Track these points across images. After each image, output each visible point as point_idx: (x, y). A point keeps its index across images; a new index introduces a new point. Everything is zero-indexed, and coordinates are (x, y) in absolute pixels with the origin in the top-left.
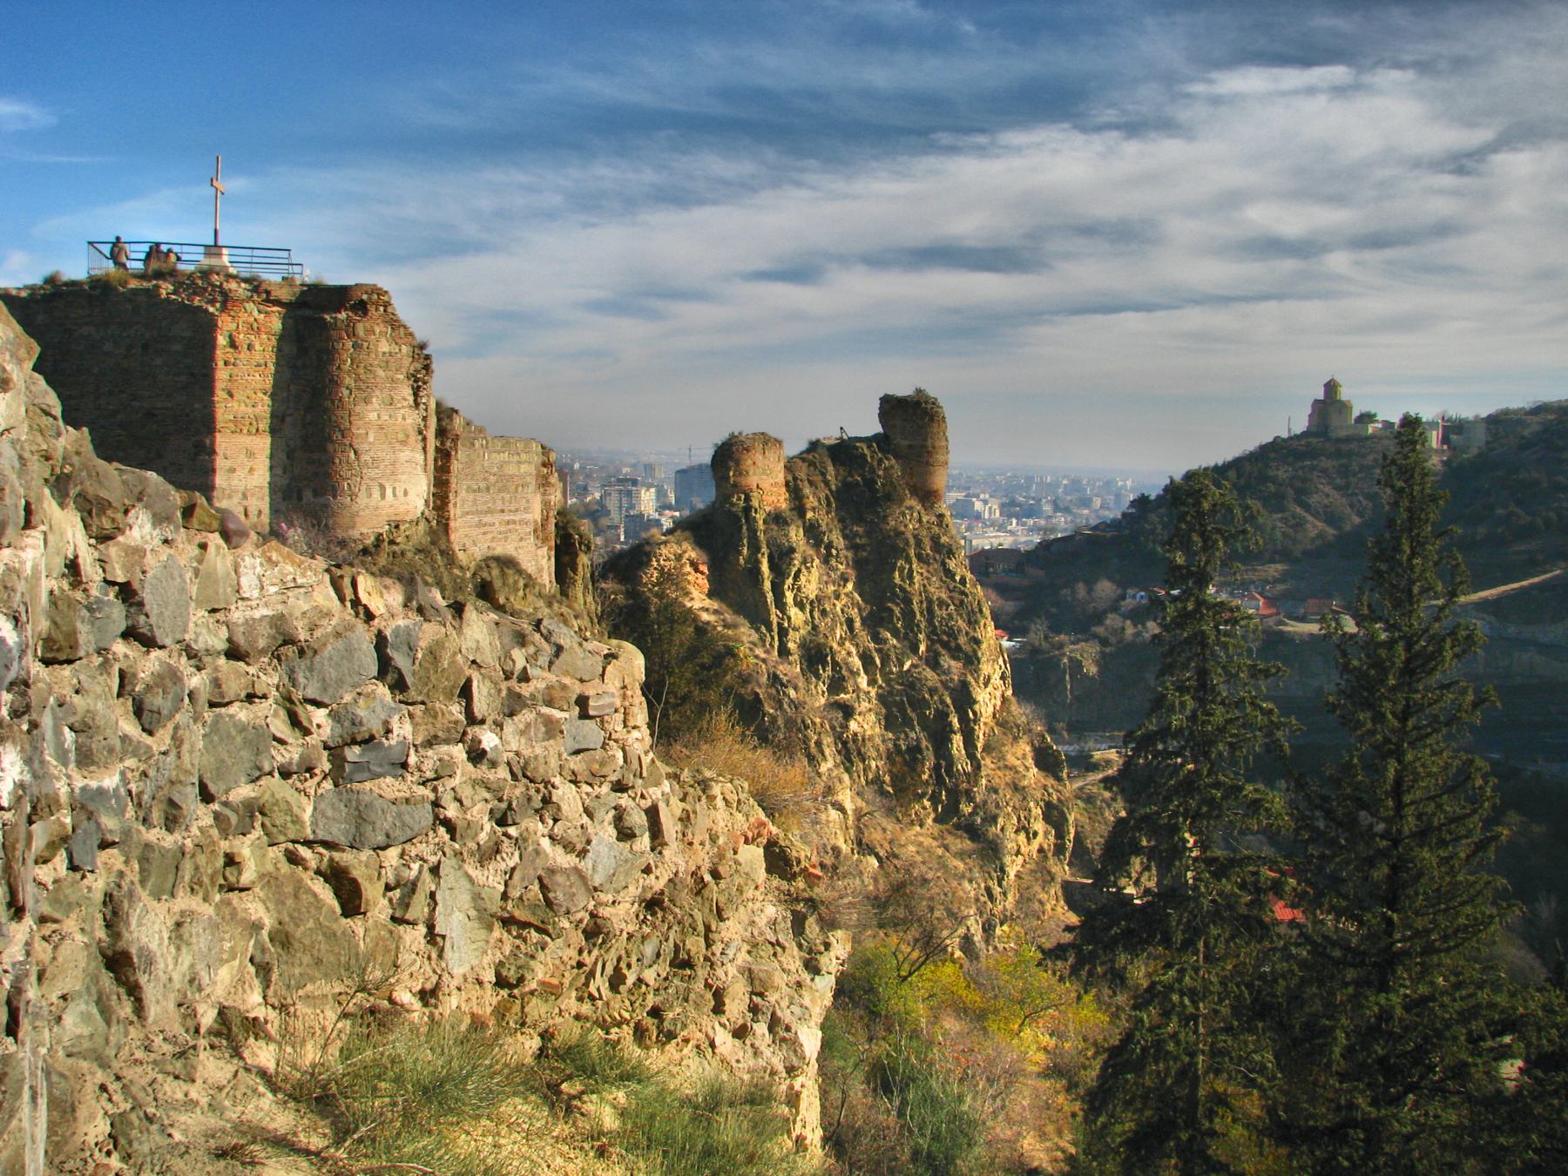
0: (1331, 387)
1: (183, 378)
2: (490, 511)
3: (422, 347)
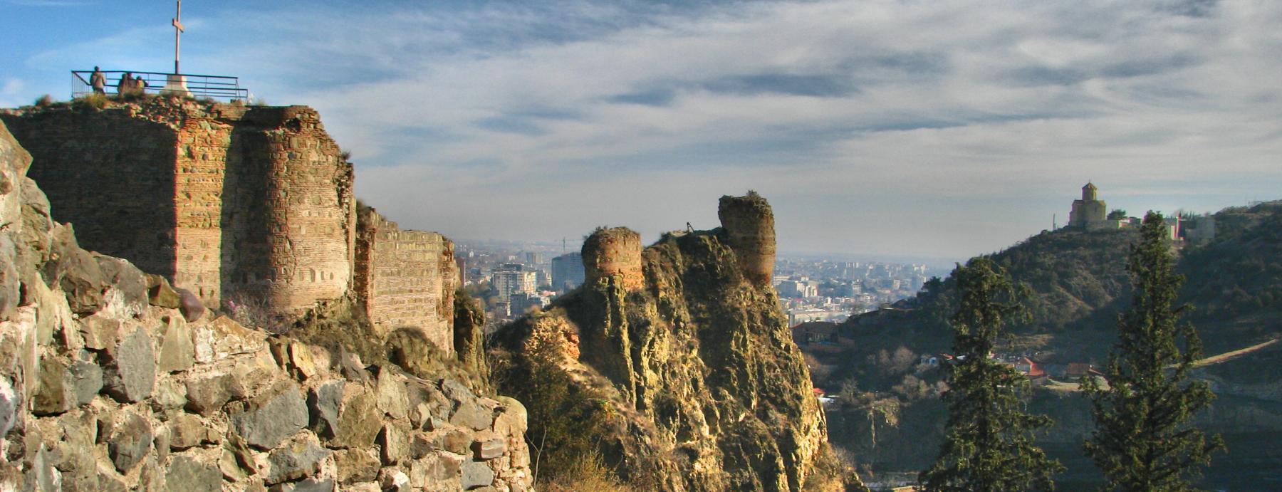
0: (1088, 190)
1: (150, 183)
2: (400, 291)
3: (345, 157)
